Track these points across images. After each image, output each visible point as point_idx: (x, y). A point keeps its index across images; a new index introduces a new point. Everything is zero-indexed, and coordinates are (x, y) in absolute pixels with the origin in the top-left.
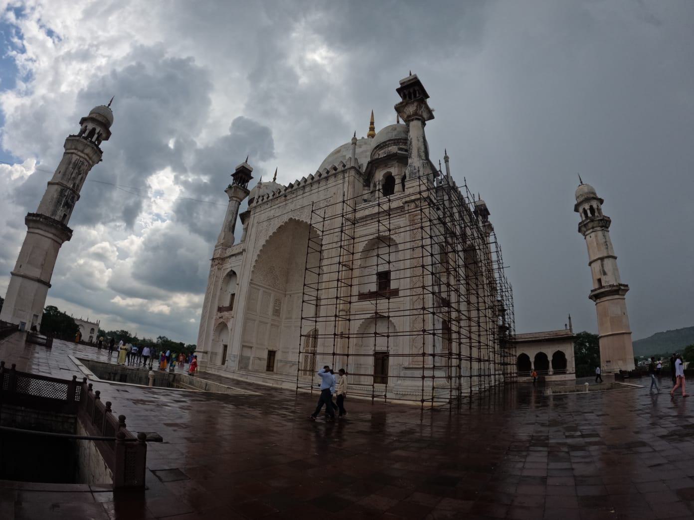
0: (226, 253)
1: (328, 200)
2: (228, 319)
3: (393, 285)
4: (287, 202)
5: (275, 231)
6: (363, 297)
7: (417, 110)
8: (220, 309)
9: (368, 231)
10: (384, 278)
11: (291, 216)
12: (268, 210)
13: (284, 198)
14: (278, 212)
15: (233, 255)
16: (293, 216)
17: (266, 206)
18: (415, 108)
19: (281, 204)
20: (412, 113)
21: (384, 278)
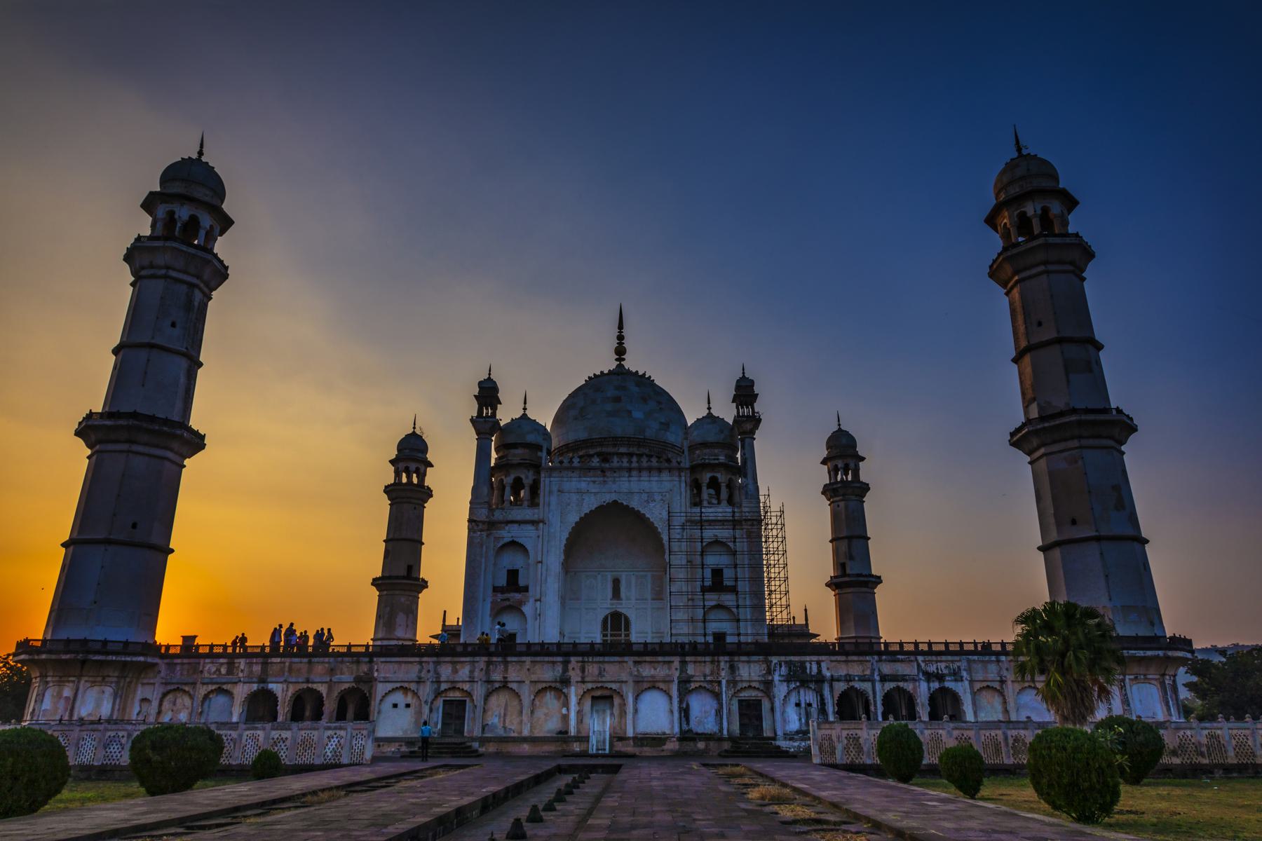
2: (521, 603)
11: (614, 497)
14: (594, 488)
17: (570, 474)
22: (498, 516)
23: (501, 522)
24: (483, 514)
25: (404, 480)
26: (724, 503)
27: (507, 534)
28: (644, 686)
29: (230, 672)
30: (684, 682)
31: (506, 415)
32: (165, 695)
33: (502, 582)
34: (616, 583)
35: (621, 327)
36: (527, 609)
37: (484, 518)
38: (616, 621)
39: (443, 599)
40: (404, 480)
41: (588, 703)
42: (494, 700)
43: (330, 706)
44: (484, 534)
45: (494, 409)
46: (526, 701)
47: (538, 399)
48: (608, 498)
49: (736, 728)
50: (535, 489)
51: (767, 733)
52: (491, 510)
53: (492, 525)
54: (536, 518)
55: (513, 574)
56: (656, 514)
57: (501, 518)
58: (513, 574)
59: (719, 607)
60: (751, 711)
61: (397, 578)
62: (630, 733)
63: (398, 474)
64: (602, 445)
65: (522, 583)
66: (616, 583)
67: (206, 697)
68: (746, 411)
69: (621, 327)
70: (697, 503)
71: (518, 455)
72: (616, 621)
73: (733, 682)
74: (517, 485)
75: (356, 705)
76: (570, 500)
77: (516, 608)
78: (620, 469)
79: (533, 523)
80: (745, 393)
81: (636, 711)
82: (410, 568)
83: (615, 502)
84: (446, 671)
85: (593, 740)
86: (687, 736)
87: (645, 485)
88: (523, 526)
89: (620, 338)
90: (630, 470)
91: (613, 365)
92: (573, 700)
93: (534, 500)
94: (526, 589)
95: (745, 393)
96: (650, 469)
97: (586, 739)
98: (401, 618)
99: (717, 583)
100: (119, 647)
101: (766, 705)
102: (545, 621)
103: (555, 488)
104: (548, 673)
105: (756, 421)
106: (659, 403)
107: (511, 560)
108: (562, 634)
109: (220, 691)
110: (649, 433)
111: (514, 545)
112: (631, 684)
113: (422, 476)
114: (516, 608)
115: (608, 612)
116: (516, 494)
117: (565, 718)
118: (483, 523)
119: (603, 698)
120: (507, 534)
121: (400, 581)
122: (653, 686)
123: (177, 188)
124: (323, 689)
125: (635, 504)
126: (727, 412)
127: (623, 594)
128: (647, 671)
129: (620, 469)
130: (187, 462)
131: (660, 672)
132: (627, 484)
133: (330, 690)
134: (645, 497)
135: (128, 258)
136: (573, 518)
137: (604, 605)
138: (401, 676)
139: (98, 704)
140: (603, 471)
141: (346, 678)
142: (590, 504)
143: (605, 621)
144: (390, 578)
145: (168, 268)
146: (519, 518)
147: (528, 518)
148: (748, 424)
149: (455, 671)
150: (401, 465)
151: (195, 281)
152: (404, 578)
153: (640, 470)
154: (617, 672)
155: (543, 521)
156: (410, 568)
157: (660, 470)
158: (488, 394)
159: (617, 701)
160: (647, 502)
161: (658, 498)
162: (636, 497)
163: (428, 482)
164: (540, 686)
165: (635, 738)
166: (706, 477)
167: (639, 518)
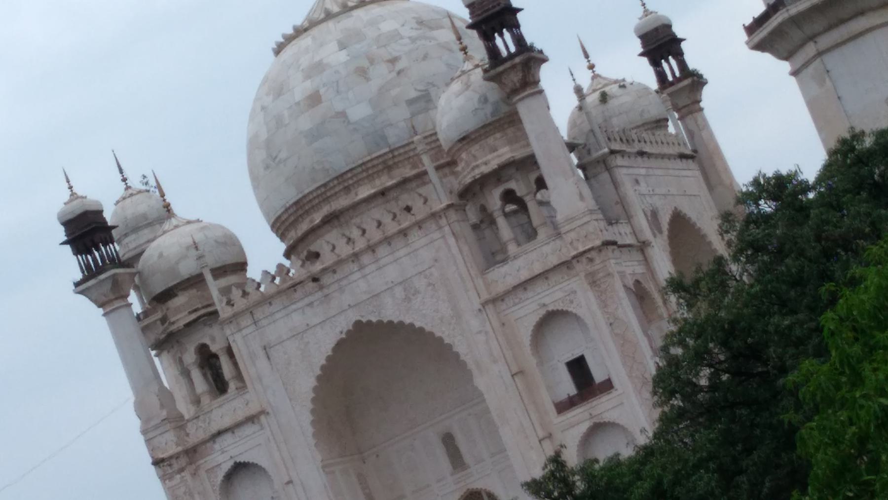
0: (188, 435)
1: (427, 272)
3: (598, 376)
4: (326, 291)
5: (330, 353)
6: (563, 407)
7: (524, 77)
9: (527, 312)
10: (578, 368)
11: (353, 316)
12: (278, 316)
13: (311, 285)
15: (220, 433)
16: (362, 317)
17: (267, 309)
18: (520, 75)
19: (311, 299)
20: (518, 85)
21: (578, 368)
22: (196, 433)
23: (204, 442)
24: (170, 445)
27: (222, 457)
37: (173, 450)
44: (186, 474)
48: (344, 324)
53: (192, 453)
54: (254, 409)
56: (424, 314)
64: (327, 200)
71: (181, 310)
78: (340, 262)
79: (251, 419)
83: (358, 324)
87: (392, 273)
88: (239, 432)
96: (387, 240)
106: (393, 61)
118: (177, 456)
120: (222, 457)
125: (391, 312)
129: (340, 262)
132: (362, 285)
134: (399, 292)
136: (306, 383)
140: (315, 280)
142: (323, 343)
146: (227, 422)
147: (240, 416)
155: (263, 412)
157: (404, 233)
160: (407, 299)
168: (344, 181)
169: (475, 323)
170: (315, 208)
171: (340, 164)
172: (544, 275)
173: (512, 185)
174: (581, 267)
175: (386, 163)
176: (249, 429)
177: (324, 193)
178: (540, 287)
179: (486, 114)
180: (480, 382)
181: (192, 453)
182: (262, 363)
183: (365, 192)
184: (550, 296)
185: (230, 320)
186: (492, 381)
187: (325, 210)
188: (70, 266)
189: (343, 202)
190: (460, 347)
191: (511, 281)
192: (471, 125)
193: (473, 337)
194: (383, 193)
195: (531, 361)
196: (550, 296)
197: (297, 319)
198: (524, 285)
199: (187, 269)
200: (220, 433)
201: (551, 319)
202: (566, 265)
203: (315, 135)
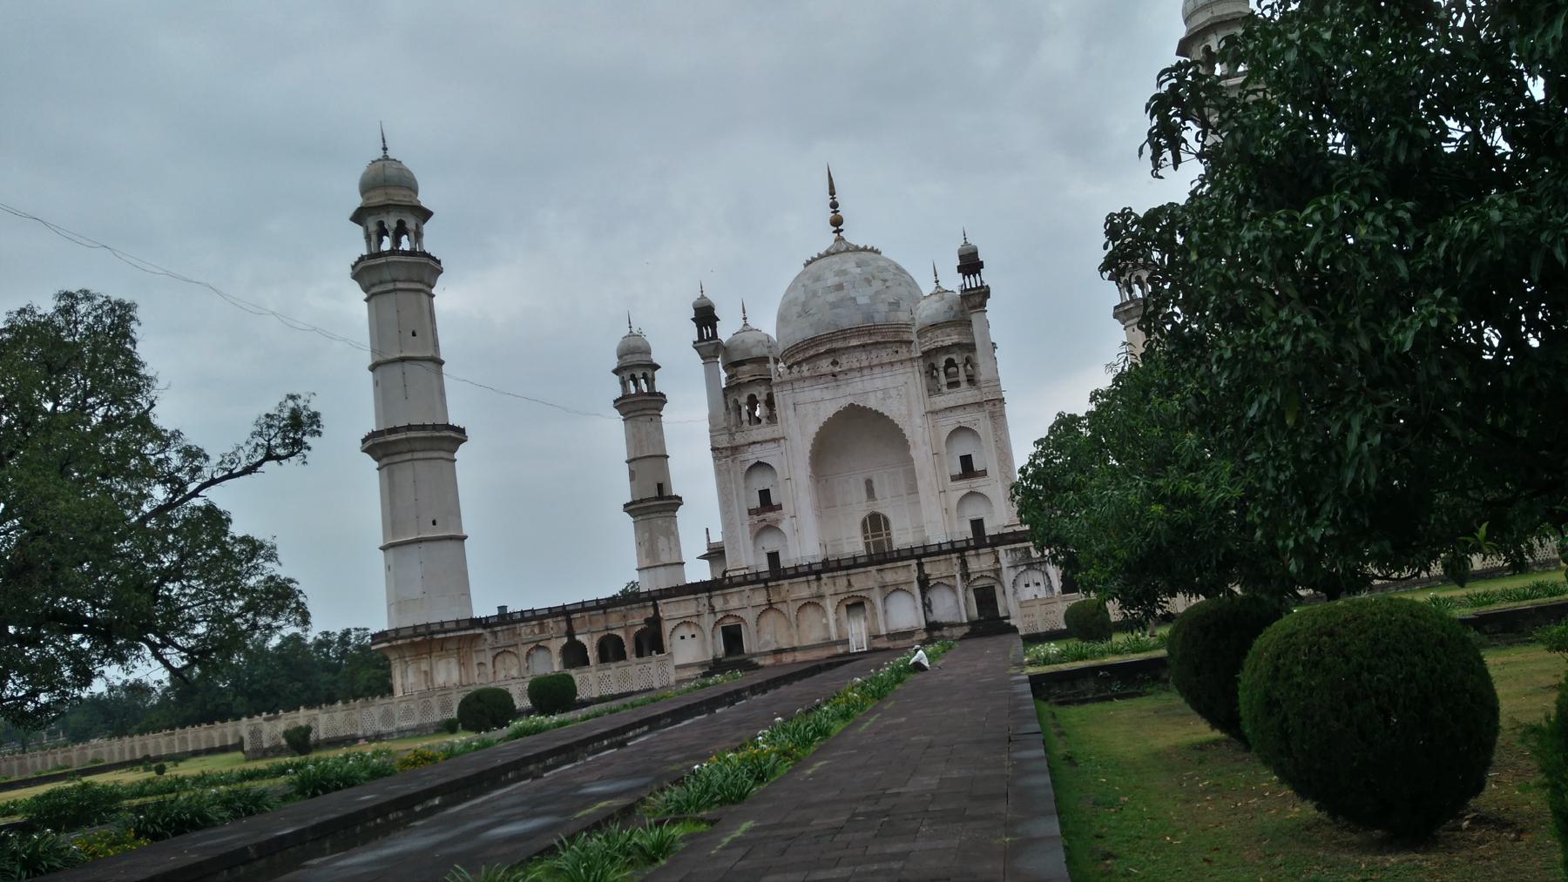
6: (954, 478)
8: (751, 512)
9: (949, 423)
11: (850, 400)
14: (827, 395)
17: (801, 384)
21: (966, 461)
22: (740, 439)
24: (724, 441)
25: (633, 390)
26: (964, 385)
27: (752, 455)
28: (890, 590)
29: (542, 631)
30: (924, 583)
31: (725, 332)
32: (495, 658)
33: (756, 503)
34: (869, 483)
35: (832, 193)
36: (784, 526)
37: (725, 445)
38: (875, 523)
39: (702, 517)
40: (633, 390)
41: (843, 610)
42: (763, 621)
43: (629, 647)
45: (714, 328)
46: (793, 619)
47: (758, 313)
48: (844, 403)
49: (974, 612)
50: (770, 403)
51: (1002, 614)
52: (731, 434)
53: (735, 450)
54: (776, 435)
55: (765, 495)
56: (893, 409)
57: (742, 441)
58: (765, 495)
59: (972, 494)
60: (986, 598)
61: (649, 500)
62: (883, 632)
63: (624, 384)
64: (831, 341)
65: (774, 501)
66: (869, 483)
67: (528, 654)
68: (972, 282)
69: (832, 193)
70: (933, 390)
71: (745, 373)
72: (875, 523)
73: (966, 575)
74: (752, 402)
75: (651, 641)
76: (808, 408)
77: (771, 528)
78: (851, 370)
79: (774, 440)
80: (970, 264)
81: (886, 612)
82: (660, 486)
84: (718, 603)
85: (853, 642)
86: (932, 627)
87: (879, 383)
89: (834, 205)
90: (861, 369)
91: (827, 240)
92: (830, 611)
93: (772, 418)
94: (780, 507)
95: (970, 264)
96: (881, 365)
97: (847, 642)
98: (662, 543)
99: (968, 469)
100: (453, 626)
101: (998, 589)
102: (803, 542)
103: (790, 403)
104: (803, 591)
105: (983, 293)
107: (761, 481)
108: (823, 545)
109: (538, 647)
110: (879, 319)
111: (760, 465)
112: (877, 590)
113: (650, 381)
114: (771, 528)
115: (865, 514)
116: (751, 413)
117: (826, 626)
119: (856, 605)
120: (752, 455)
121: (655, 505)
122: (897, 589)
123: (378, 198)
124: (621, 633)
125: (873, 403)
126: (954, 282)
127: (877, 495)
128: (890, 577)
129: (851, 370)
130: (456, 455)
131: (901, 576)
132: (860, 385)
133: (627, 633)
134: (880, 394)
135: (356, 277)
136: (813, 428)
137: (861, 511)
138: (682, 613)
139: (449, 674)
141: (638, 619)
142: (829, 410)
143: (864, 524)
144: (642, 501)
145: (394, 281)
146: (759, 438)
147: (768, 437)
148: (976, 298)
149: (726, 602)
150: (627, 375)
151: (419, 286)
152: (656, 499)
153: (871, 367)
154: (865, 581)
156: (660, 486)
157: (892, 364)
158: (705, 316)
159: (867, 606)
161: (893, 393)
162: (872, 396)
163: (659, 387)
164: (800, 603)
165: (888, 635)
166: (941, 362)
167: (880, 416)
168: (844, 333)
169: (918, 421)
170: (821, 344)
171: (845, 324)
172: (964, 406)
173: (953, 356)
174: (988, 407)
175: (869, 331)
176: (772, 445)
177: (831, 337)
178: (959, 412)
179: (950, 316)
180: (913, 453)
181: (735, 450)
182: (791, 413)
183: (854, 342)
184: (965, 418)
185: (778, 384)
186: (921, 454)
187: (828, 346)
188: (692, 332)
189: (840, 344)
190: (907, 432)
191: (944, 405)
192: (941, 319)
193: (917, 429)
194: (863, 346)
195: (944, 449)
196: (965, 418)
197: (817, 394)
198: (951, 409)
199: (756, 352)
200: (750, 444)
201: (961, 430)
202: (979, 404)
203: (834, 305)
